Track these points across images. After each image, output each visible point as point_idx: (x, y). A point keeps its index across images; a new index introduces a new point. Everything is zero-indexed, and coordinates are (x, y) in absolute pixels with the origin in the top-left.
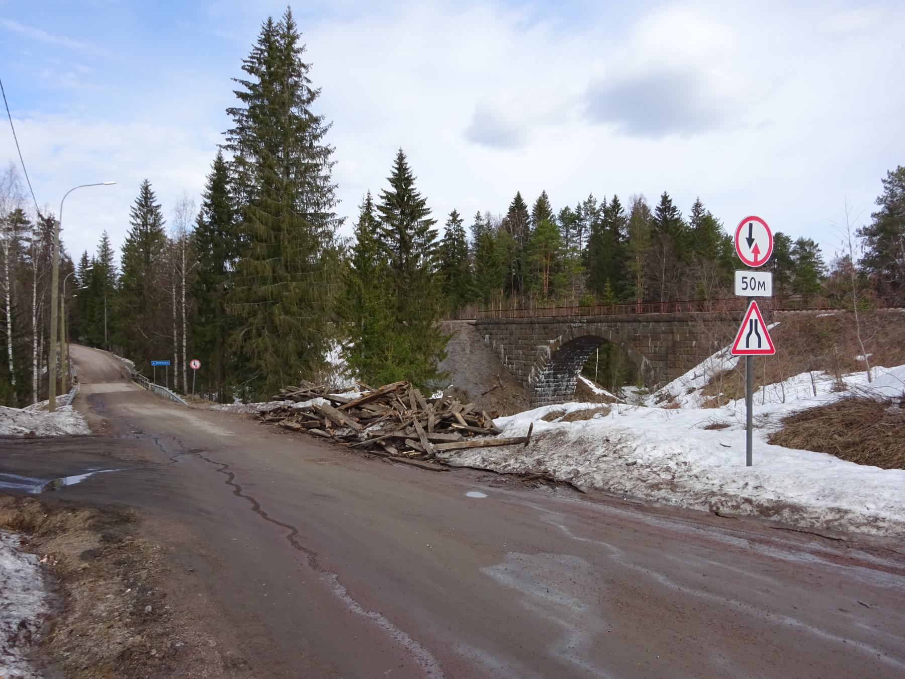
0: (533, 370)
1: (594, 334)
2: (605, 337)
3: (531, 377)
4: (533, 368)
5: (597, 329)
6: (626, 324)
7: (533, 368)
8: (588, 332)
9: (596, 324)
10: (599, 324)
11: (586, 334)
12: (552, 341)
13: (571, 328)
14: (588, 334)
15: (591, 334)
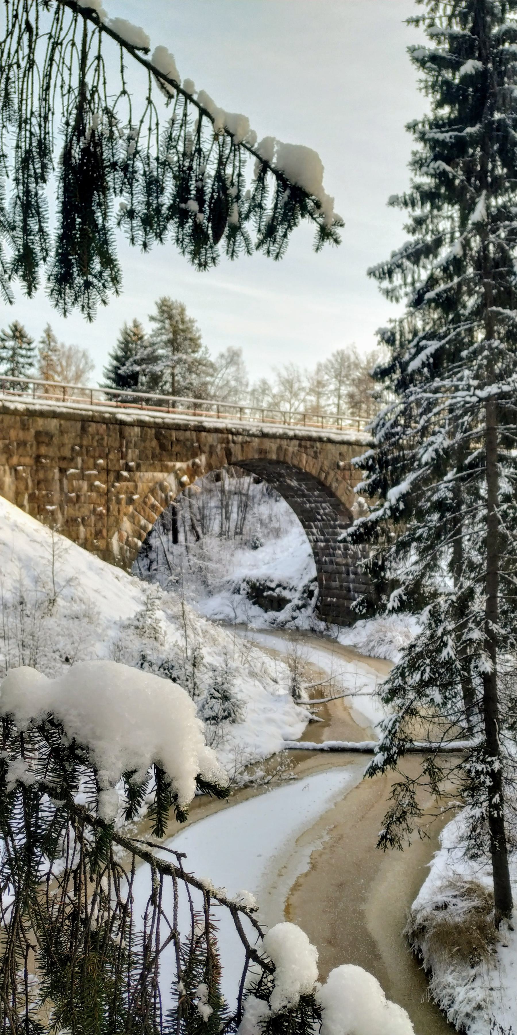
0: (127, 525)
1: (274, 457)
2: (296, 462)
3: (120, 539)
4: (125, 519)
5: (280, 448)
6: (330, 446)
7: (125, 519)
8: (261, 451)
9: (278, 440)
10: (284, 443)
11: (256, 456)
12: (179, 465)
13: (228, 442)
14: (262, 456)
15: (269, 456)
